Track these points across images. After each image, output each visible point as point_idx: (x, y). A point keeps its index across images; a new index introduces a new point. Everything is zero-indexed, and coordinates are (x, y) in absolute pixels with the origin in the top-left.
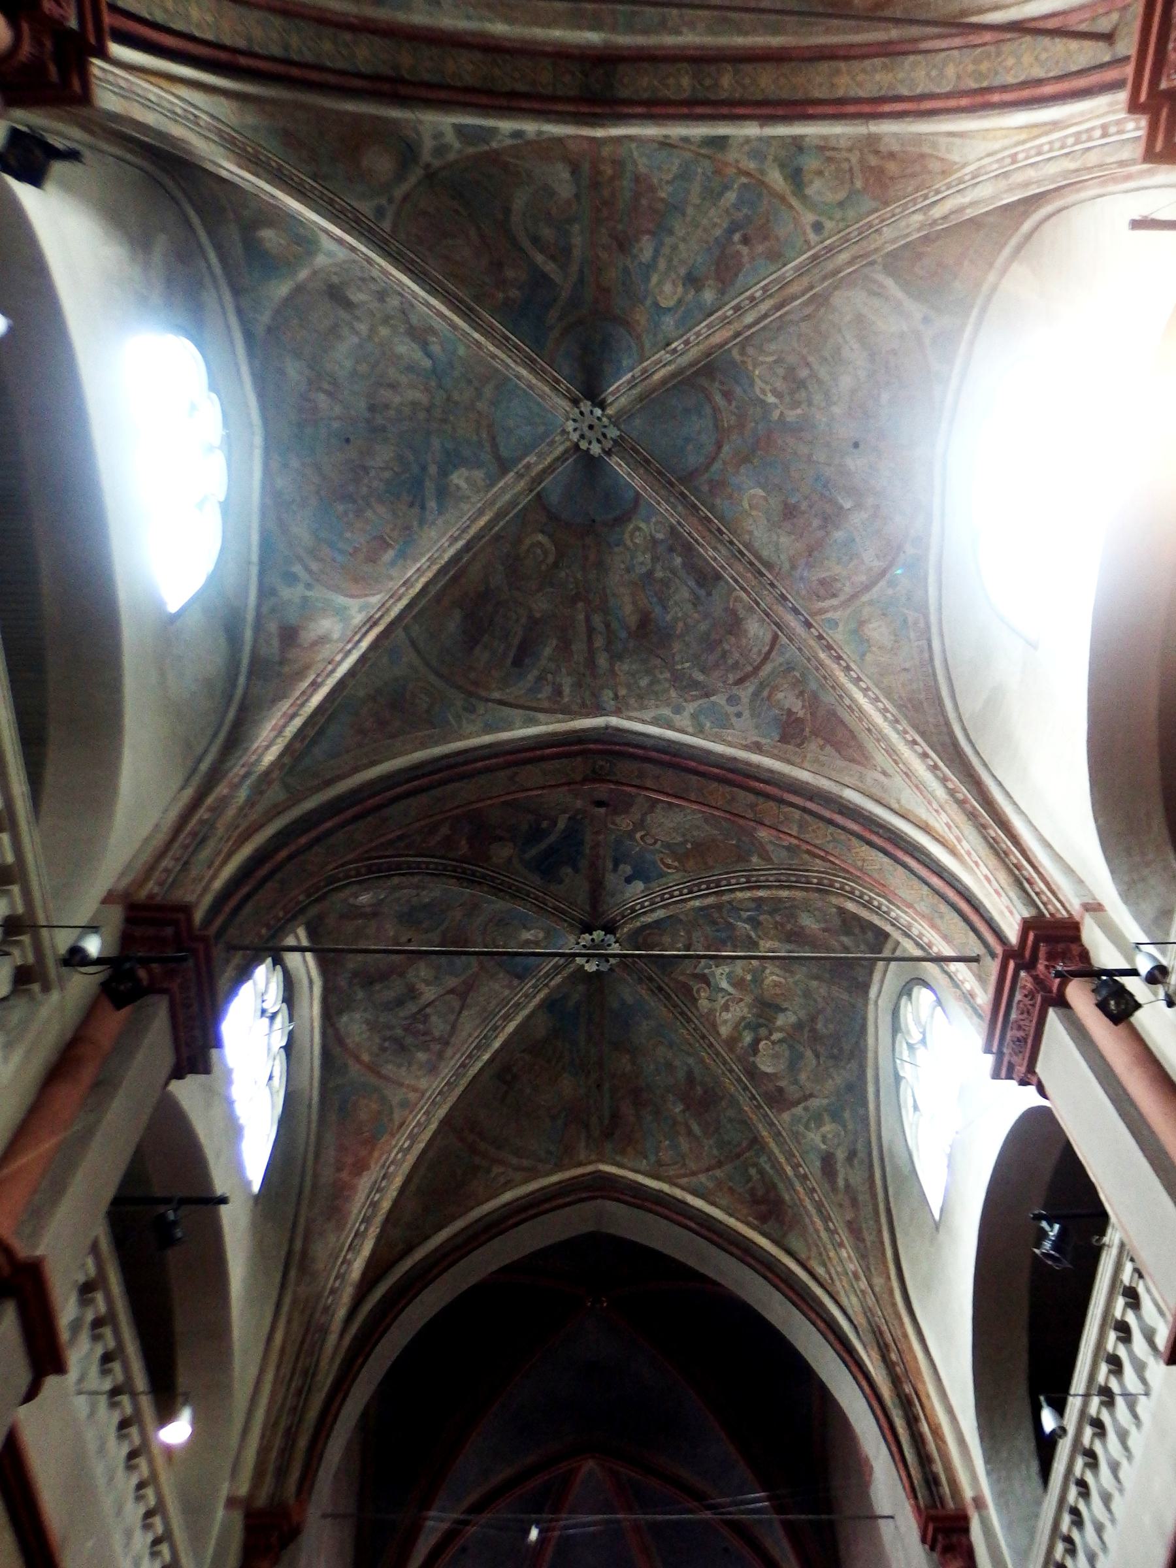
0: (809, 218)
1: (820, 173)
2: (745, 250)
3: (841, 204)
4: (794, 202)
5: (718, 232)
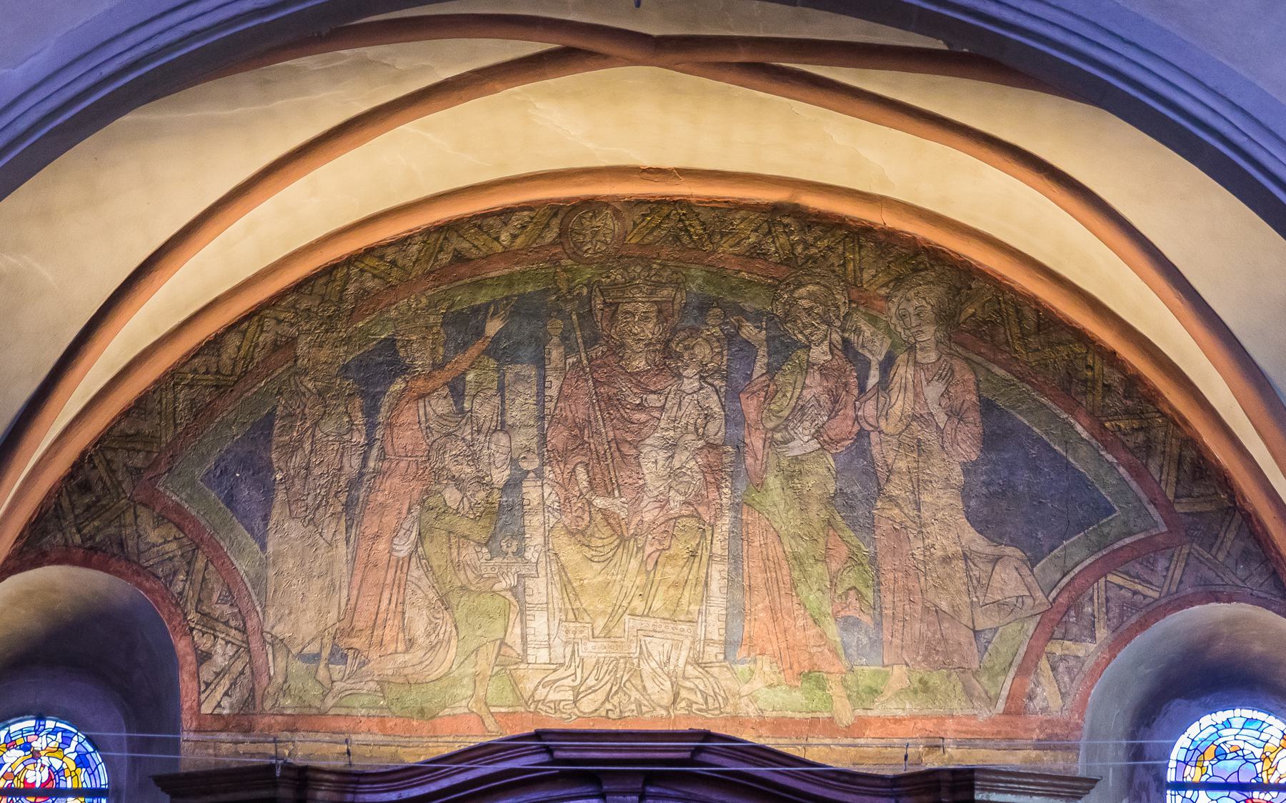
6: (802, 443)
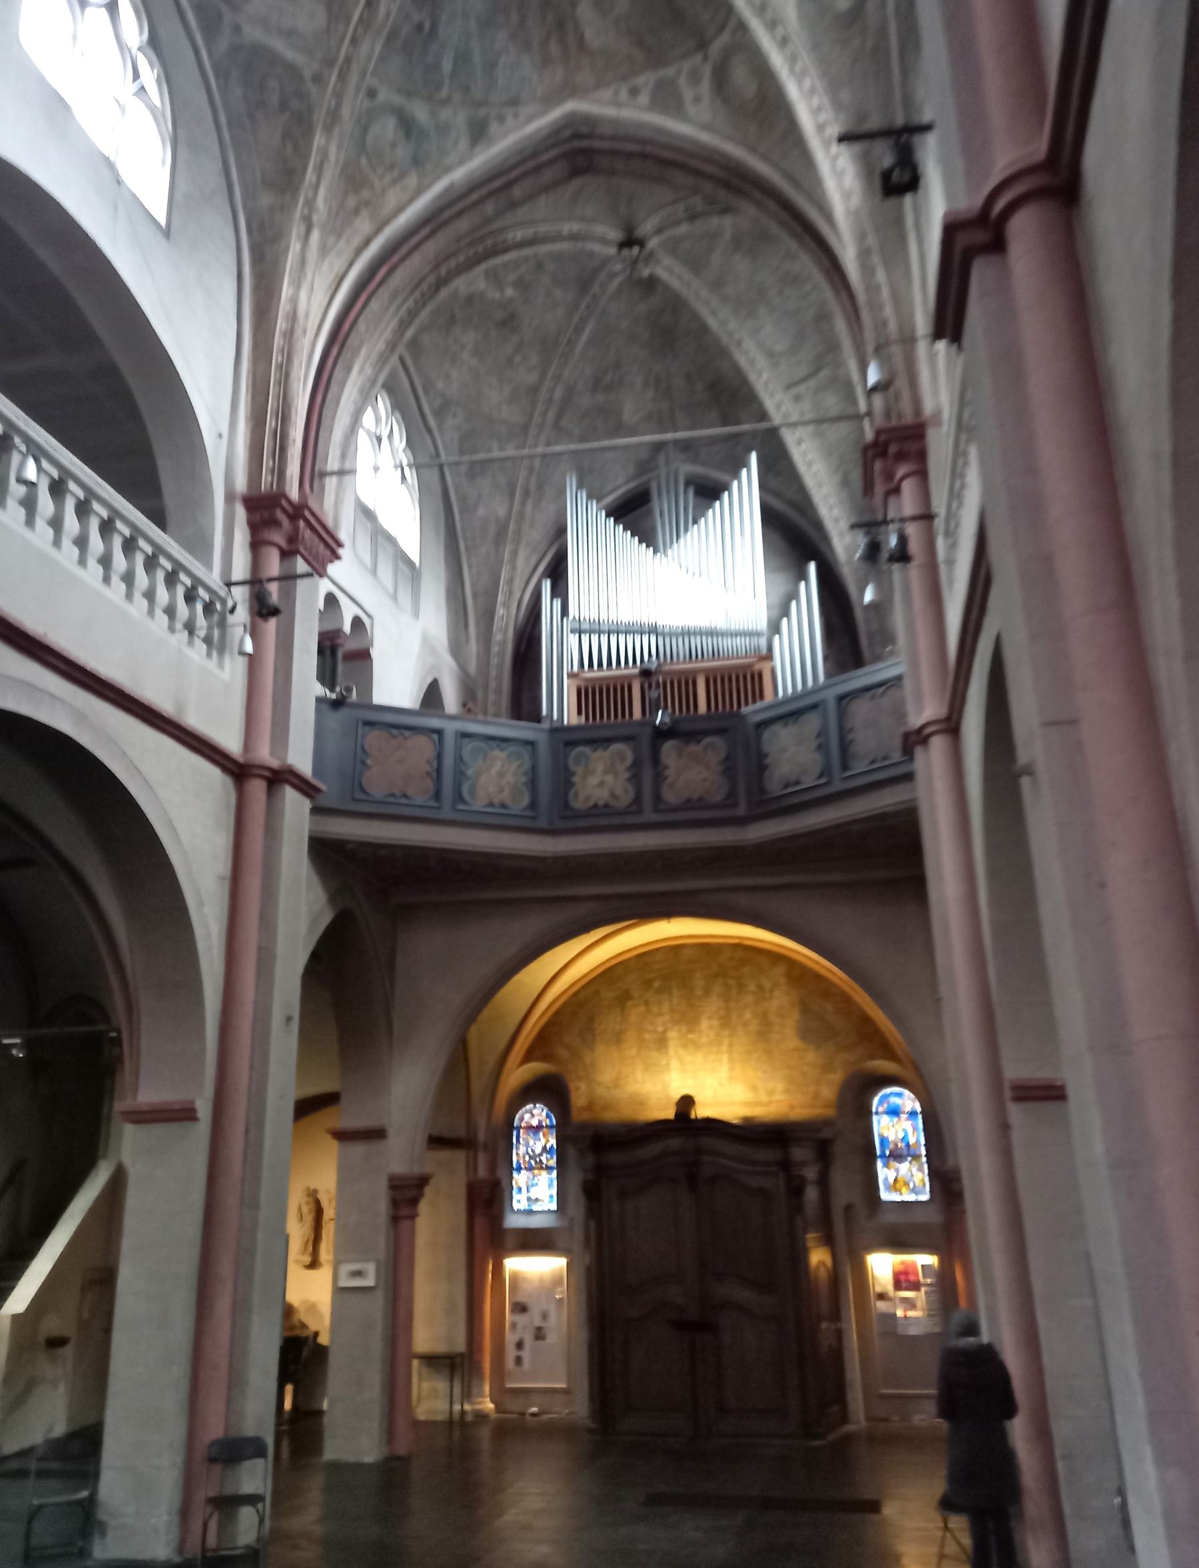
0: (383, 96)
1: (393, 146)
2: (416, 17)
3: (365, 129)
4: (398, 100)
5: (444, 17)
6: (748, 1015)
